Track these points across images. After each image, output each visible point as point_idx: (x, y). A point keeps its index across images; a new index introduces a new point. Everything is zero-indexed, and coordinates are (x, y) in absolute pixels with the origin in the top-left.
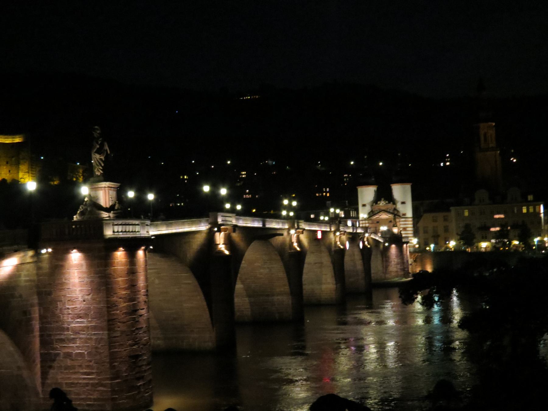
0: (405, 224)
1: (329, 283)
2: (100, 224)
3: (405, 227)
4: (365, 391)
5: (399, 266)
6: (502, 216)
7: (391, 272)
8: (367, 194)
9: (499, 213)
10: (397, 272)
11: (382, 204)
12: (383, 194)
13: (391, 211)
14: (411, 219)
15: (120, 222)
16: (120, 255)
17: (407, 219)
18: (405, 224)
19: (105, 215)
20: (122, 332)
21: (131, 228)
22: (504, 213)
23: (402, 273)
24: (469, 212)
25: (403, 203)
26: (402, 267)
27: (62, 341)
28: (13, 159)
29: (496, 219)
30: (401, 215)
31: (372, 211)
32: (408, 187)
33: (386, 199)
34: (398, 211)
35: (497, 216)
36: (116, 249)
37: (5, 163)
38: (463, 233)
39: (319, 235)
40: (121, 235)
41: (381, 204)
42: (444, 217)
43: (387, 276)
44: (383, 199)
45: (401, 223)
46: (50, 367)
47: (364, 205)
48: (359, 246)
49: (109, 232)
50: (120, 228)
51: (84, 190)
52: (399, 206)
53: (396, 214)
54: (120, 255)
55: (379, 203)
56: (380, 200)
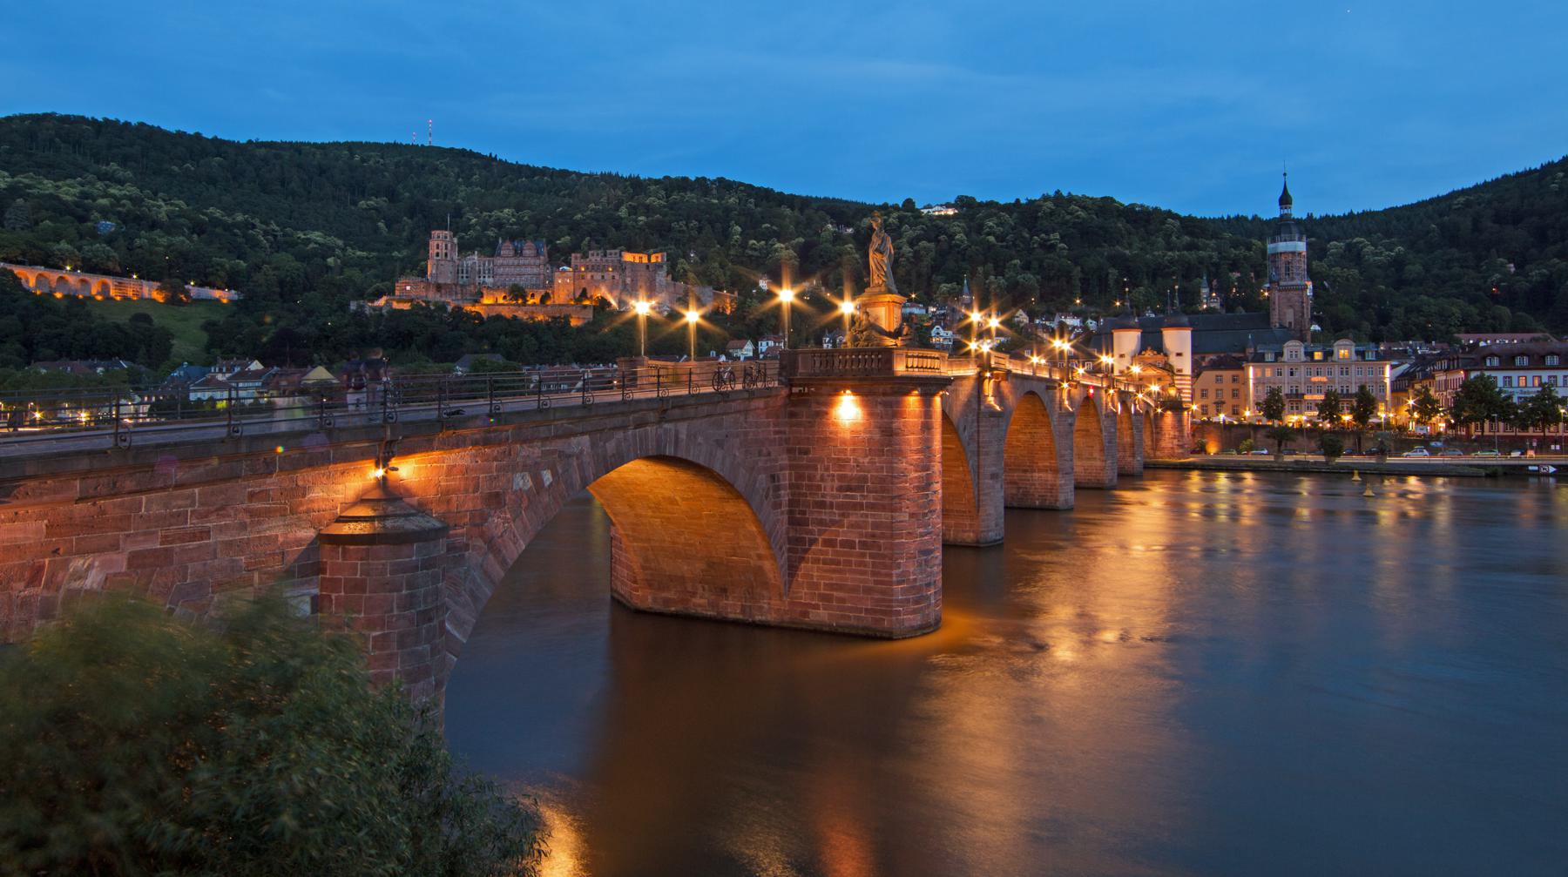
2: (887, 356)
3: (1184, 387)
12: (1152, 342)
15: (916, 353)
16: (913, 401)
19: (890, 342)
20: (912, 515)
21: (929, 363)
25: (1179, 354)
27: (821, 522)
32: (1187, 334)
33: (1153, 349)
36: (908, 393)
38: (1267, 402)
40: (917, 373)
46: (802, 559)
49: (900, 368)
50: (916, 362)
51: (847, 307)
52: (1173, 360)
53: (1168, 368)
54: (913, 401)
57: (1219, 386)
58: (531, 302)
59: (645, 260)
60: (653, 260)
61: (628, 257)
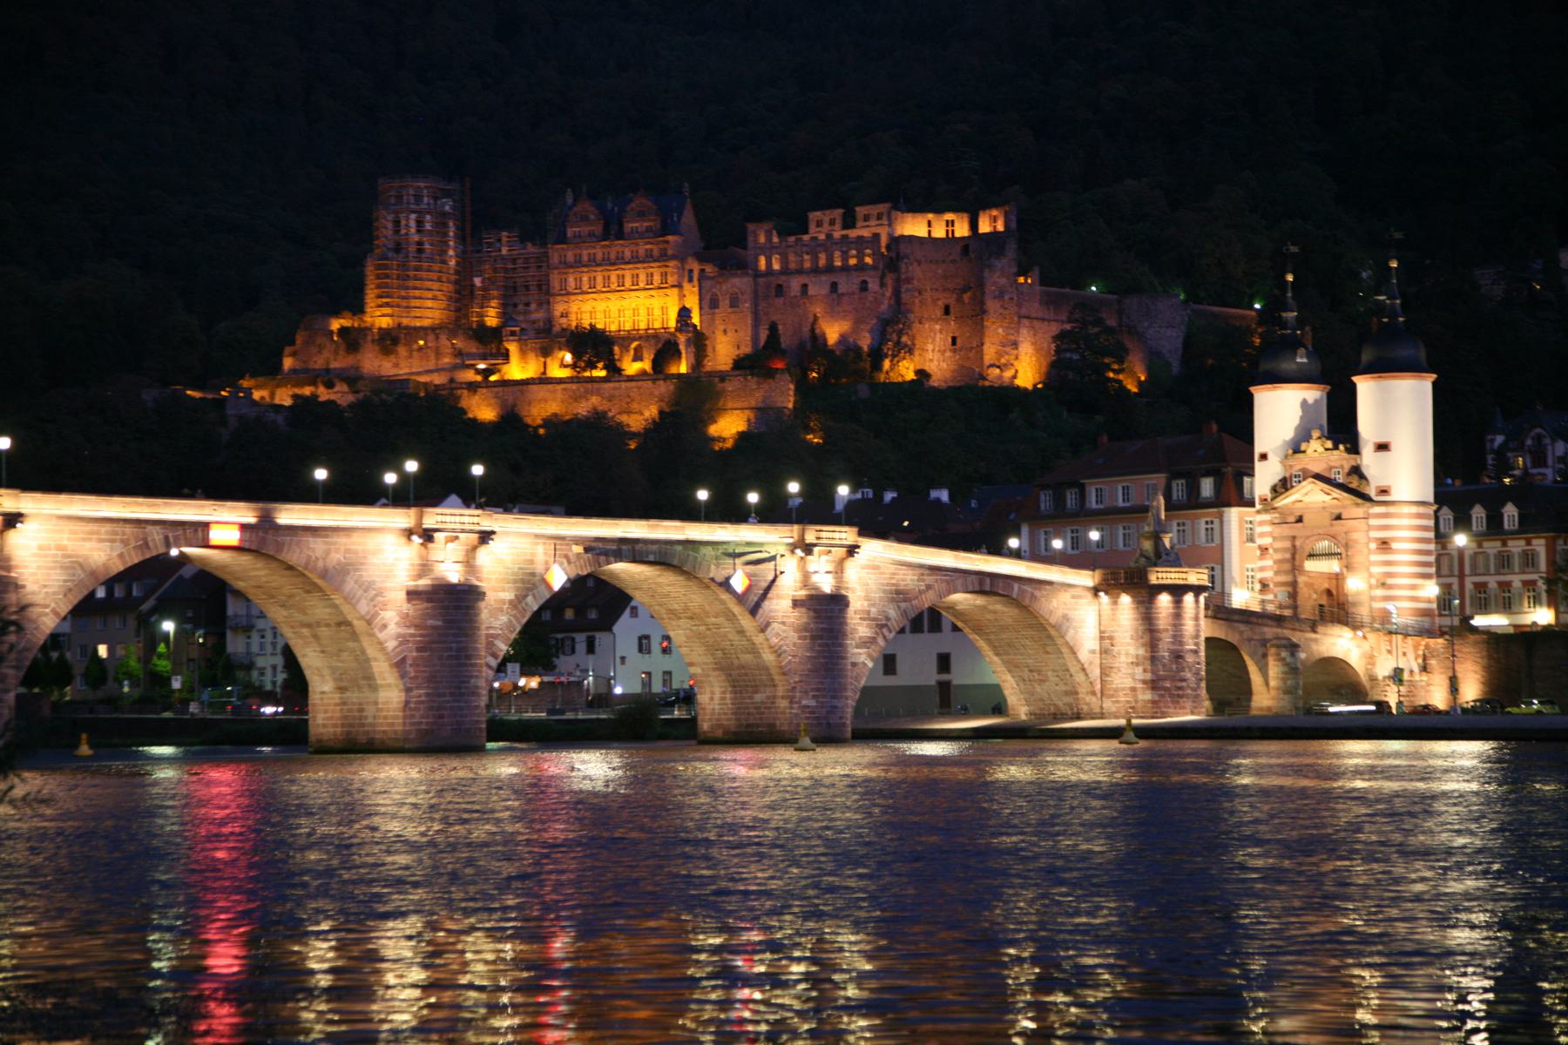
0: (1386, 528)
1: (389, 685)
4: (194, 993)
5: (1139, 670)
7: (1116, 690)
8: (1280, 411)
10: (1133, 689)
13: (1341, 479)
17: (1391, 509)
18: (1386, 528)
23: (1148, 696)
25: (1382, 447)
26: (1148, 676)
28: (966, 297)
30: (1372, 493)
34: (1362, 477)
37: (939, 313)
39: (219, 535)
43: (1108, 705)
45: (1373, 522)
47: (1264, 457)
48: (725, 584)
52: (1368, 459)
53: (1354, 486)
56: (1308, 438)
58: (632, 367)
59: (962, 230)
60: (985, 227)
61: (915, 226)
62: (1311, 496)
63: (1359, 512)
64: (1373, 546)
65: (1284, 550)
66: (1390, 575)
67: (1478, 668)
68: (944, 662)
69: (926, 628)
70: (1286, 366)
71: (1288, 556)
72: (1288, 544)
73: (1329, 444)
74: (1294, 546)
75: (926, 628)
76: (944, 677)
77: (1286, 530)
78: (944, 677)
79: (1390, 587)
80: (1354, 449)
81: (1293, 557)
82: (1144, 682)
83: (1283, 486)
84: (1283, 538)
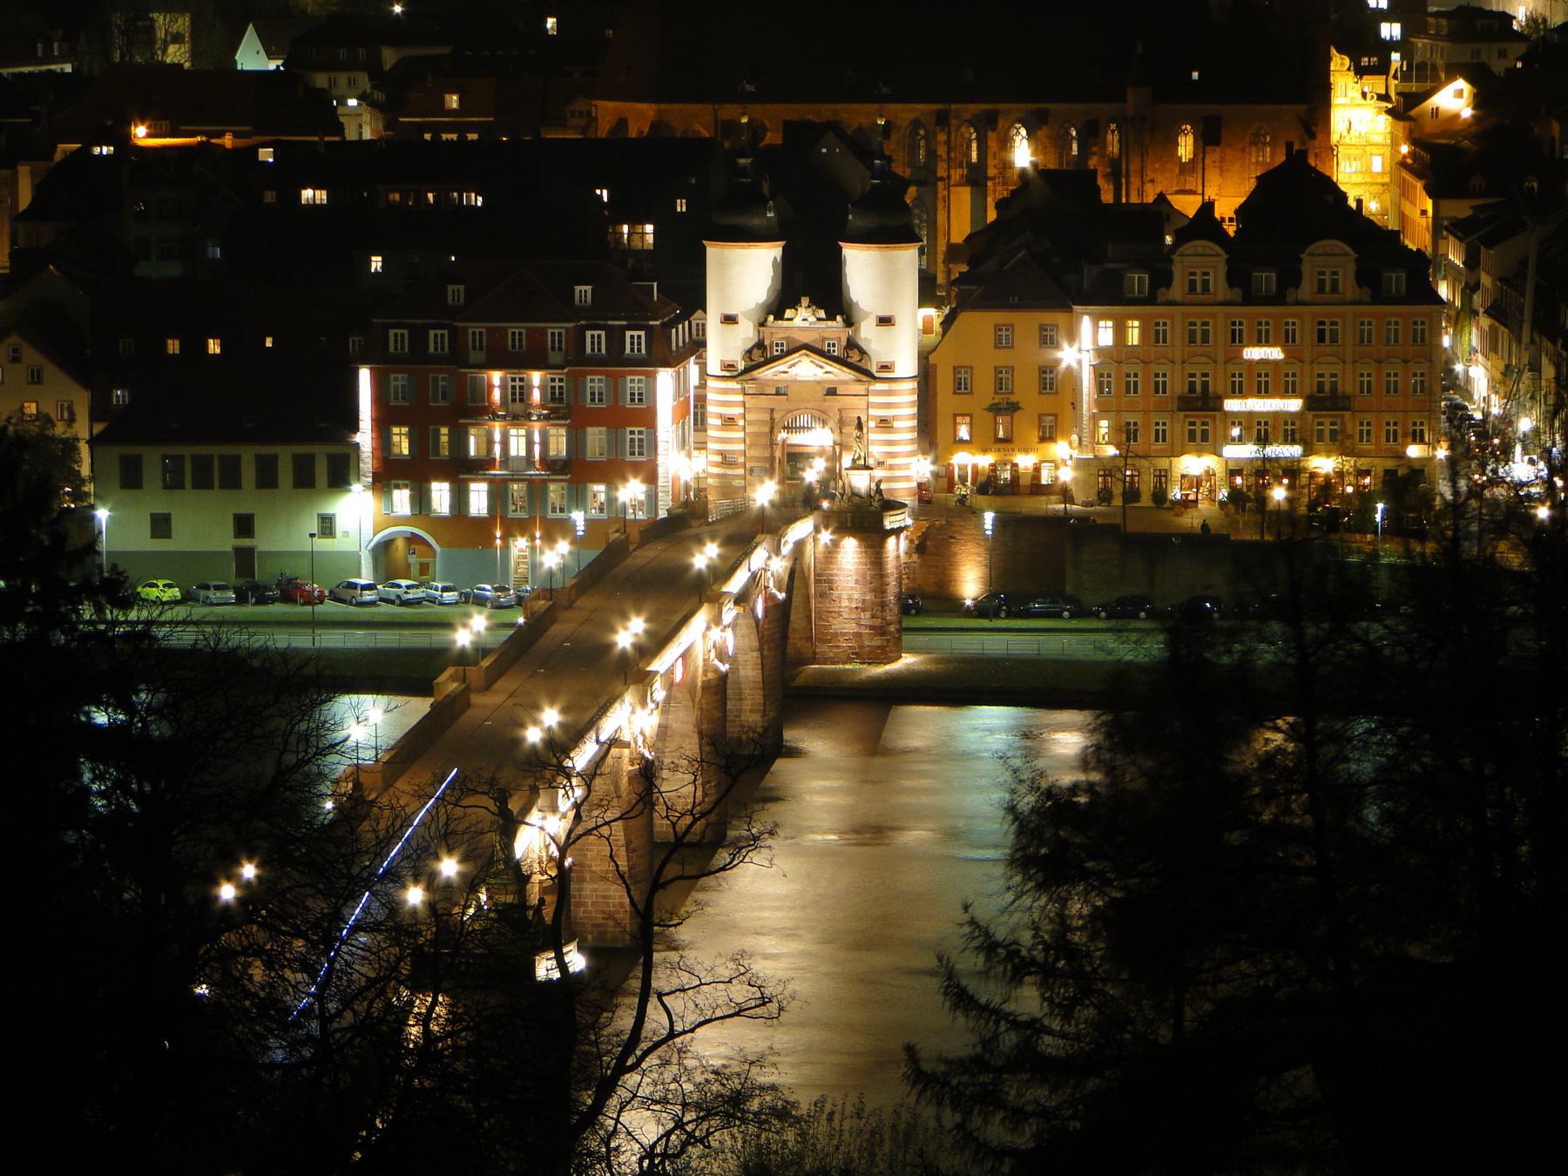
0: (889, 406)
6: (1275, 353)
7: (836, 635)
8: (744, 273)
9: (1260, 341)
10: (858, 635)
11: (803, 319)
12: (811, 280)
14: (913, 385)
17: (895, 386)
18: (889, 406)
22: (1286, 341)
23: (877, 642)
24: (1143, 329)
25: (885, 321)
29: (1251, 363)
30: (874, 370)
31: (760, 345)
33: (816, 303)
34: (863, 352)
35: (1253, 353)
41: (798, 322)
42: (1043, 328)
44: (805, 301)
47: (730, 319)
52: (868, 332)
55: (789, 313)
56: (794, 304)
57: (1003, 358)
62: (806, 369)
63: (860, 389)
64: (872, 424)
65: (763, 422)
66: (892, 455)
67: (981, 550)
68: (244, 525)
69: (216, 484)
70: (756, 222)
71: (767, 429)
72: (767, 417)
73: (822, 314)
74: (772, 419)
75: (216, 484)
76: (245, 542)
77: (764, 402)
78: (245, 542)
79: (891, 467)
80: (849, 323)
81: (772, 431)
82: (871, 627)
83: (760, 355)
84: (760, 409)
